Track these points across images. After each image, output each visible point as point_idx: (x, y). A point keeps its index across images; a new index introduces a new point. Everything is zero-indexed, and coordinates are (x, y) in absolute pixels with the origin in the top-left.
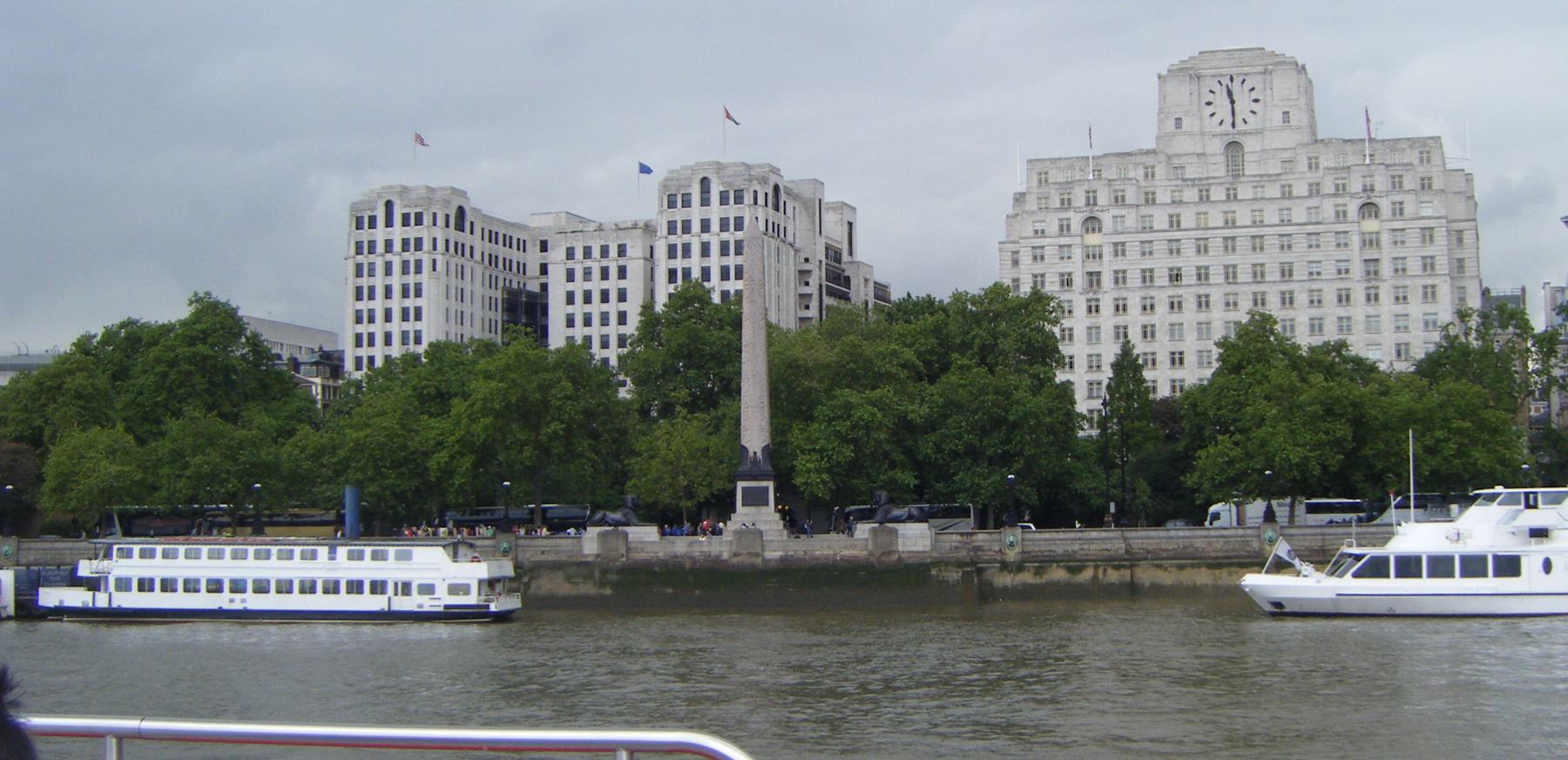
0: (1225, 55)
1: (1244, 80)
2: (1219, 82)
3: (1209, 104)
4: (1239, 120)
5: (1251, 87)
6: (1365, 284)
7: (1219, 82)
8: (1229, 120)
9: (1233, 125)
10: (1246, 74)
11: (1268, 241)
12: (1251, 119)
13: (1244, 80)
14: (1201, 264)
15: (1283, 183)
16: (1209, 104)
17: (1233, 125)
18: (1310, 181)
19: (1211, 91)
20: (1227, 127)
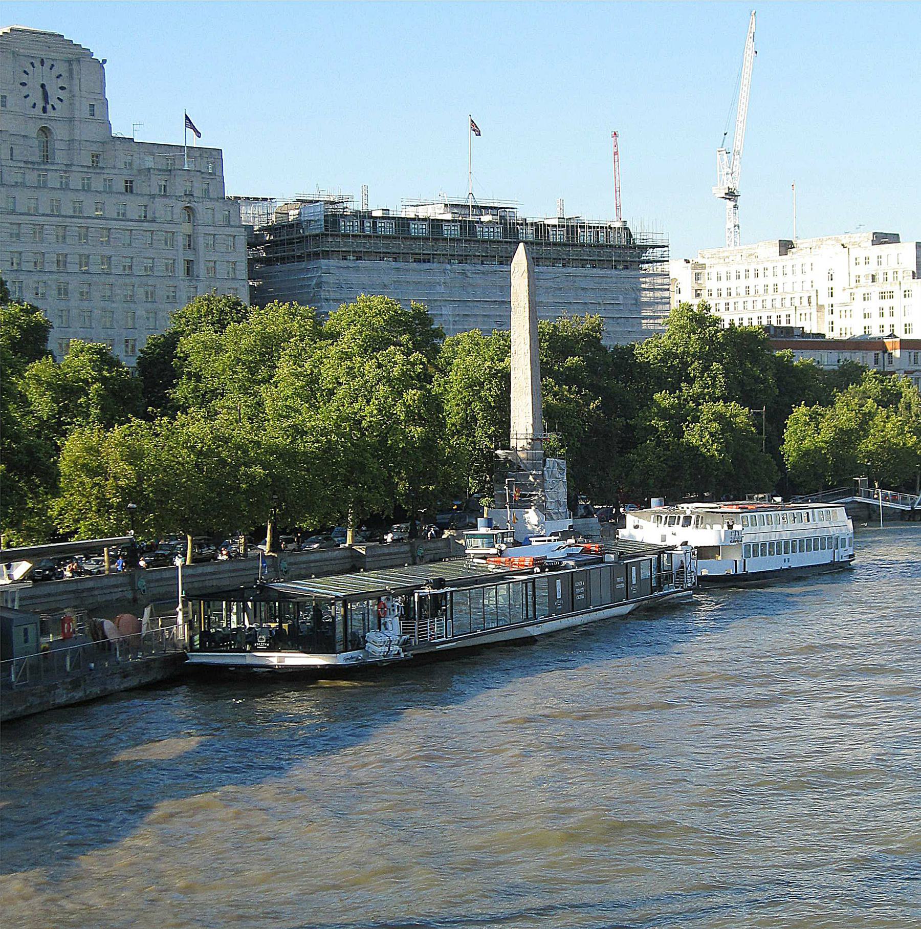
0: (32, 37)
1: (53, 65)
2: (32, 63)
3: (24, 84)
4: (49, 107)
5: (57, 74)
6: (187, 283)
7: (32, 63)
8: (40, 104)
9: (45, 110)
10: (53, 60)
11: (92, 233)
12: (58, 105)
13: (53, 65)
14: (61, 251)
15: (106, 176)
16: (24, 84)
17: (45, 110)
18: (127, 178)
19: (25, 72)
20: (38, 111)
